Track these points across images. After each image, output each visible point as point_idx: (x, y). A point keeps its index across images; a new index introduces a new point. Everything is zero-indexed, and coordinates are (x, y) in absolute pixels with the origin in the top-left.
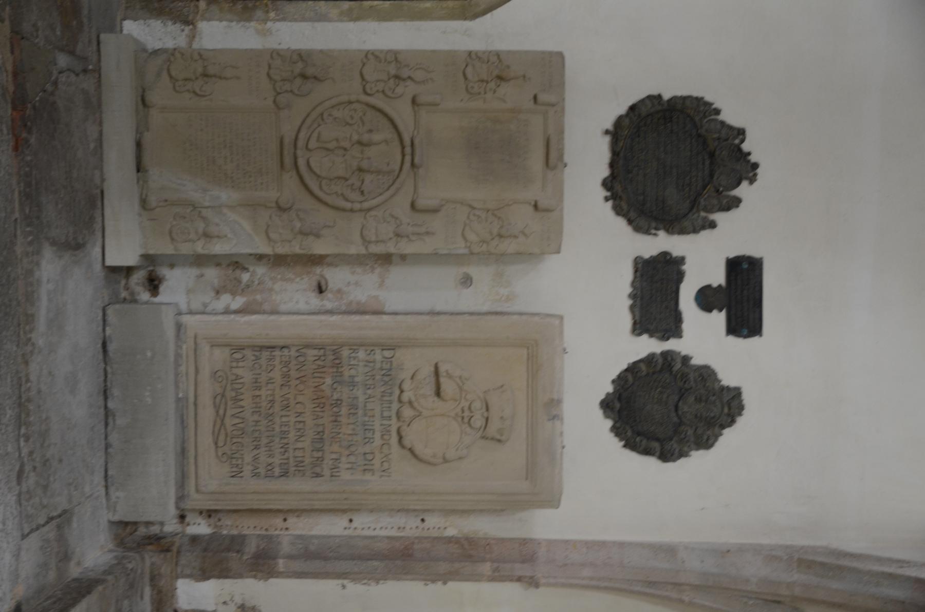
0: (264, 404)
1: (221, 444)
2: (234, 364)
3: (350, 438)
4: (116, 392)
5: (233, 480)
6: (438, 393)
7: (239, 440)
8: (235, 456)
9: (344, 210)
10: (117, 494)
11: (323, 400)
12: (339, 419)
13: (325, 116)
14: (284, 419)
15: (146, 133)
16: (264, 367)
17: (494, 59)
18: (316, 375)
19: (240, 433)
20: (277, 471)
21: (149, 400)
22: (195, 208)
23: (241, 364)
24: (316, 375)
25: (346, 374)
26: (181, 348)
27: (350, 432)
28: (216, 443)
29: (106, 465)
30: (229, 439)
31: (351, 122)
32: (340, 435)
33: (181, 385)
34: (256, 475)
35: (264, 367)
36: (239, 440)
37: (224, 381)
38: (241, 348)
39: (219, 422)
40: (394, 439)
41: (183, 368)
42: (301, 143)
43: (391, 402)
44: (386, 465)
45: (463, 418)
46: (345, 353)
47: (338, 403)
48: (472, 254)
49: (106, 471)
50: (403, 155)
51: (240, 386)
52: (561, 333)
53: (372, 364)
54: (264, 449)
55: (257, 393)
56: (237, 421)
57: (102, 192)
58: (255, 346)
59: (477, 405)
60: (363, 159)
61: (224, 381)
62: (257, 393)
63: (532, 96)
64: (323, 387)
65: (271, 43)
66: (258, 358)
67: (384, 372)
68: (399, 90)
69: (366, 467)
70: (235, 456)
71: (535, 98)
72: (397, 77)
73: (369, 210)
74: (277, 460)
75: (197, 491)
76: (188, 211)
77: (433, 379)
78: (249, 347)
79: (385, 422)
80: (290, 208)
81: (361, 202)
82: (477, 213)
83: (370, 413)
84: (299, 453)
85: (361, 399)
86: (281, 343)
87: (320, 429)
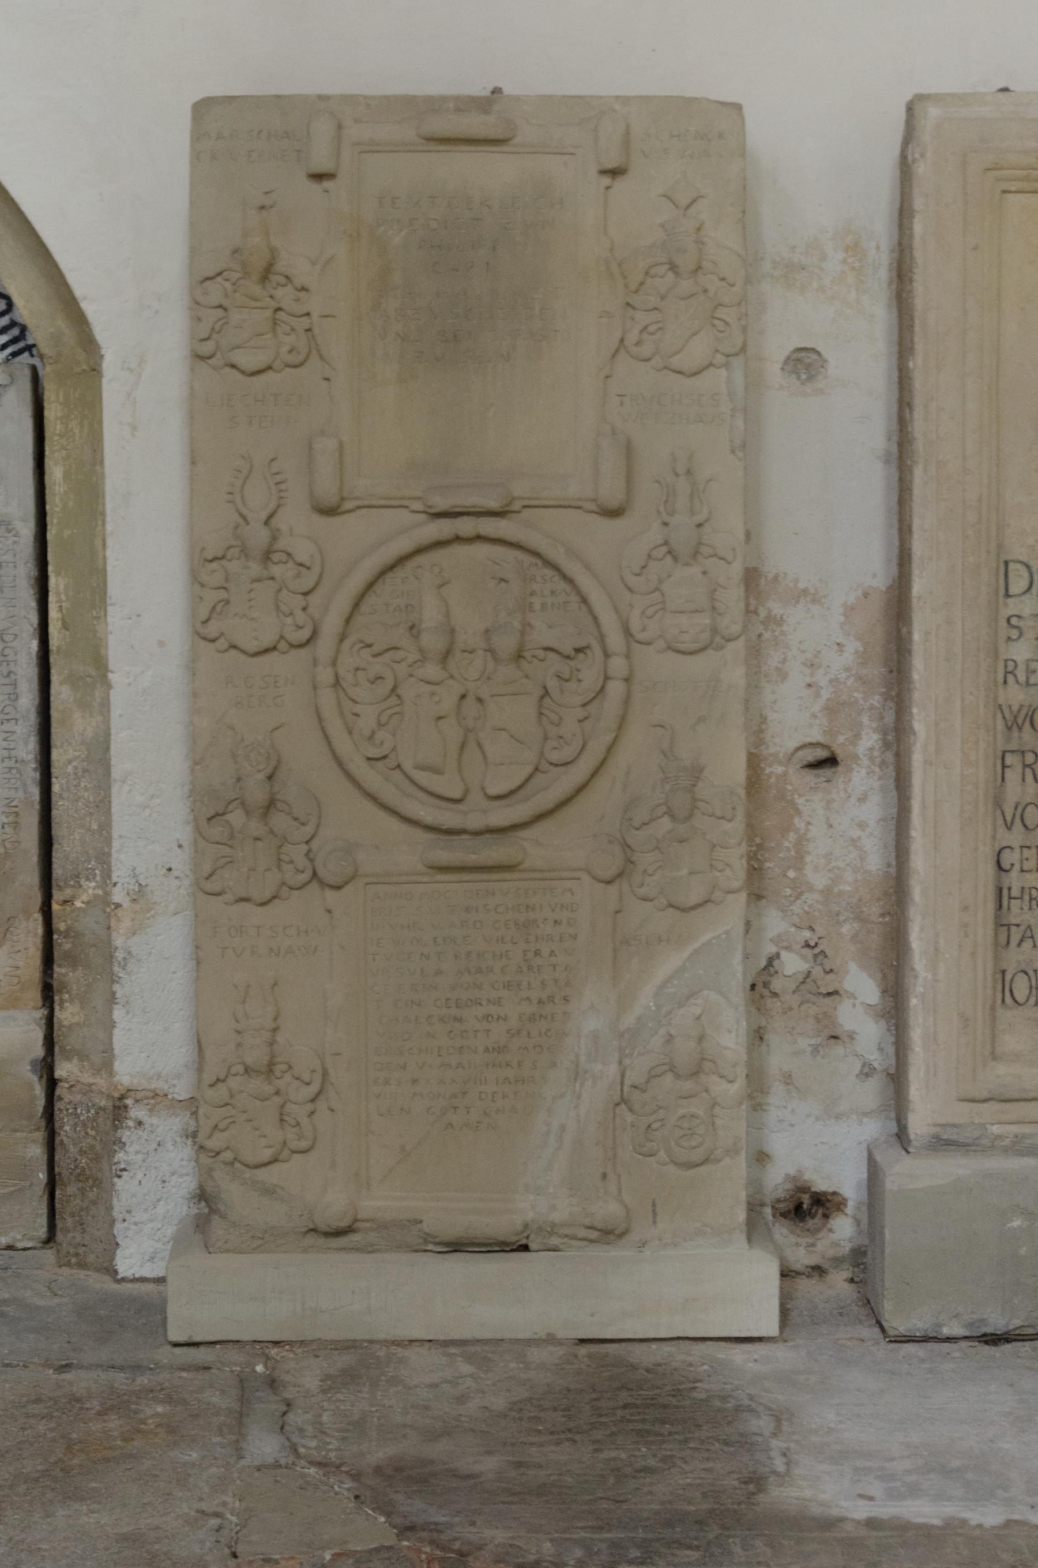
9: (627, 702)
13: (374, 752)
15: (424, 1226)
17: (215, 292)
22: (623, 1100)
26: (998, 1137)
31: (389, 684)
42: (448, 818)
46: (1015, 696)
48: (743, 349)
50: (479, 538)
52: (961, 99)
57: (582, 1341)
58: (996, 944)
60: (490, 650)
63: (315, 187)
65: (173, 896)
68: (303, 551)
71: (319, 177)
72: (267, 557)
73: (627, 632)
76: (630, 1118)
78: (996, 959)
80: (626, 846)
81: (607, 655)
82: (633, 336)
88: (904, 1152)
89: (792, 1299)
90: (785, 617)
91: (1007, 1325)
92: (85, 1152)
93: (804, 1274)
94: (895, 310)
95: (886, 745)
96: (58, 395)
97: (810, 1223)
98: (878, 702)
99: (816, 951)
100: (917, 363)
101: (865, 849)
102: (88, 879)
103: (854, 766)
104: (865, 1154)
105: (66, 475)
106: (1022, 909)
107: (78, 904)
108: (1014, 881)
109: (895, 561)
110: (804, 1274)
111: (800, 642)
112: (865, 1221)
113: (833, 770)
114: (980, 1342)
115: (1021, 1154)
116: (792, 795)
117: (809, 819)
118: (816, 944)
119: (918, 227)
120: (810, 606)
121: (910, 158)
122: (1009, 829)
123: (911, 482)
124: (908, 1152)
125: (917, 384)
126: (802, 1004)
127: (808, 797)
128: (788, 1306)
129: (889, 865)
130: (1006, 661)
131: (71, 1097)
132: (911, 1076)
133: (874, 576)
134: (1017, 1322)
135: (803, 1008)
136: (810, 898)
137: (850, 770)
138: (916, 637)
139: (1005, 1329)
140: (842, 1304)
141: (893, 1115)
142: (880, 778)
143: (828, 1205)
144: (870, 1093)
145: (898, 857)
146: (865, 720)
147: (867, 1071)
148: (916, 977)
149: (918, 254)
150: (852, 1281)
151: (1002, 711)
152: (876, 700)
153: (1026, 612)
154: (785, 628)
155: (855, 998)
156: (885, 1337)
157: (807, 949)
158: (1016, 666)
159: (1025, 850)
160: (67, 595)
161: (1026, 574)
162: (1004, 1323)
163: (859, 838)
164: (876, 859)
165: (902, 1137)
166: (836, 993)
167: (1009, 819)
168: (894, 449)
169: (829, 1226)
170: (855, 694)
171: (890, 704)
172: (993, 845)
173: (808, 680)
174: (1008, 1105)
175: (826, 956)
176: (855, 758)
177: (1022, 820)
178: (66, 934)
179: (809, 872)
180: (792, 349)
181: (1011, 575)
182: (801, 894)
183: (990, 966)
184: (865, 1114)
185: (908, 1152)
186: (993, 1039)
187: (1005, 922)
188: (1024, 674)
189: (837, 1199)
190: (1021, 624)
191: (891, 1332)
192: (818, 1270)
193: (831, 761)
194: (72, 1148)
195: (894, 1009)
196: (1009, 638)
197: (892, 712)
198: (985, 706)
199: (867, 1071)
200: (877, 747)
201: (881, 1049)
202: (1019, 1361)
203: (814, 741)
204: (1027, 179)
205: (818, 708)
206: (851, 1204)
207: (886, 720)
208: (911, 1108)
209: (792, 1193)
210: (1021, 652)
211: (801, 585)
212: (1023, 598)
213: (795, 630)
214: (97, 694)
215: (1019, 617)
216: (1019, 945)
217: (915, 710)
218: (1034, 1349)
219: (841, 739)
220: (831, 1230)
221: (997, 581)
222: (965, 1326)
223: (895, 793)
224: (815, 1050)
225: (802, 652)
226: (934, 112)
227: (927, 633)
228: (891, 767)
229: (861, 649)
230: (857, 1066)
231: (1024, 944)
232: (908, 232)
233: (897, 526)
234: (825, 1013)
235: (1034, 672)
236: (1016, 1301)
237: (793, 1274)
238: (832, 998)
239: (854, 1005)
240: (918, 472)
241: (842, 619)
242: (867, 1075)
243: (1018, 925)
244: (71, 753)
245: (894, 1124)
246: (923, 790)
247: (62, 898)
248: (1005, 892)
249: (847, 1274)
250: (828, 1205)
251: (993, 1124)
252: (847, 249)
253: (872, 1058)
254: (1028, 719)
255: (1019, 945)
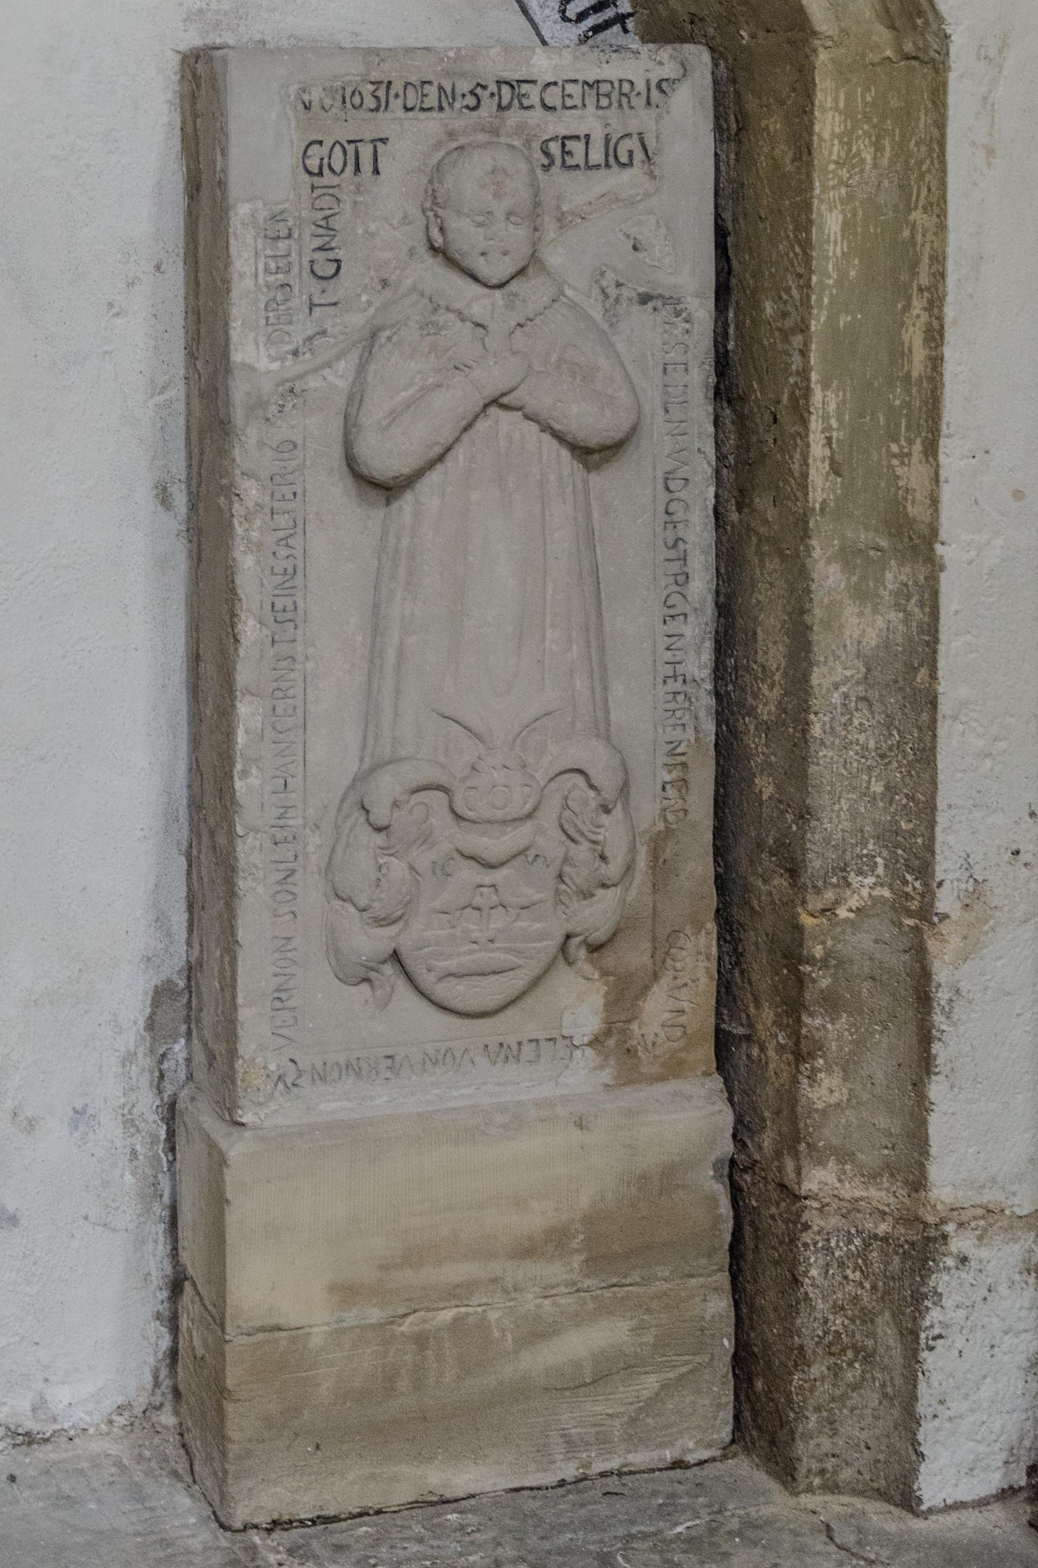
92: (842, 1308)
96: (836, 100)
102: (860, 873)
105: (847, 226)
107: (842, 913)
131: (822, 1223)
160: (840, 420)
178: (824, 963)
194: (820, 1305)
214: (889, 576)
244: (840, 673)
247: (820, 906)
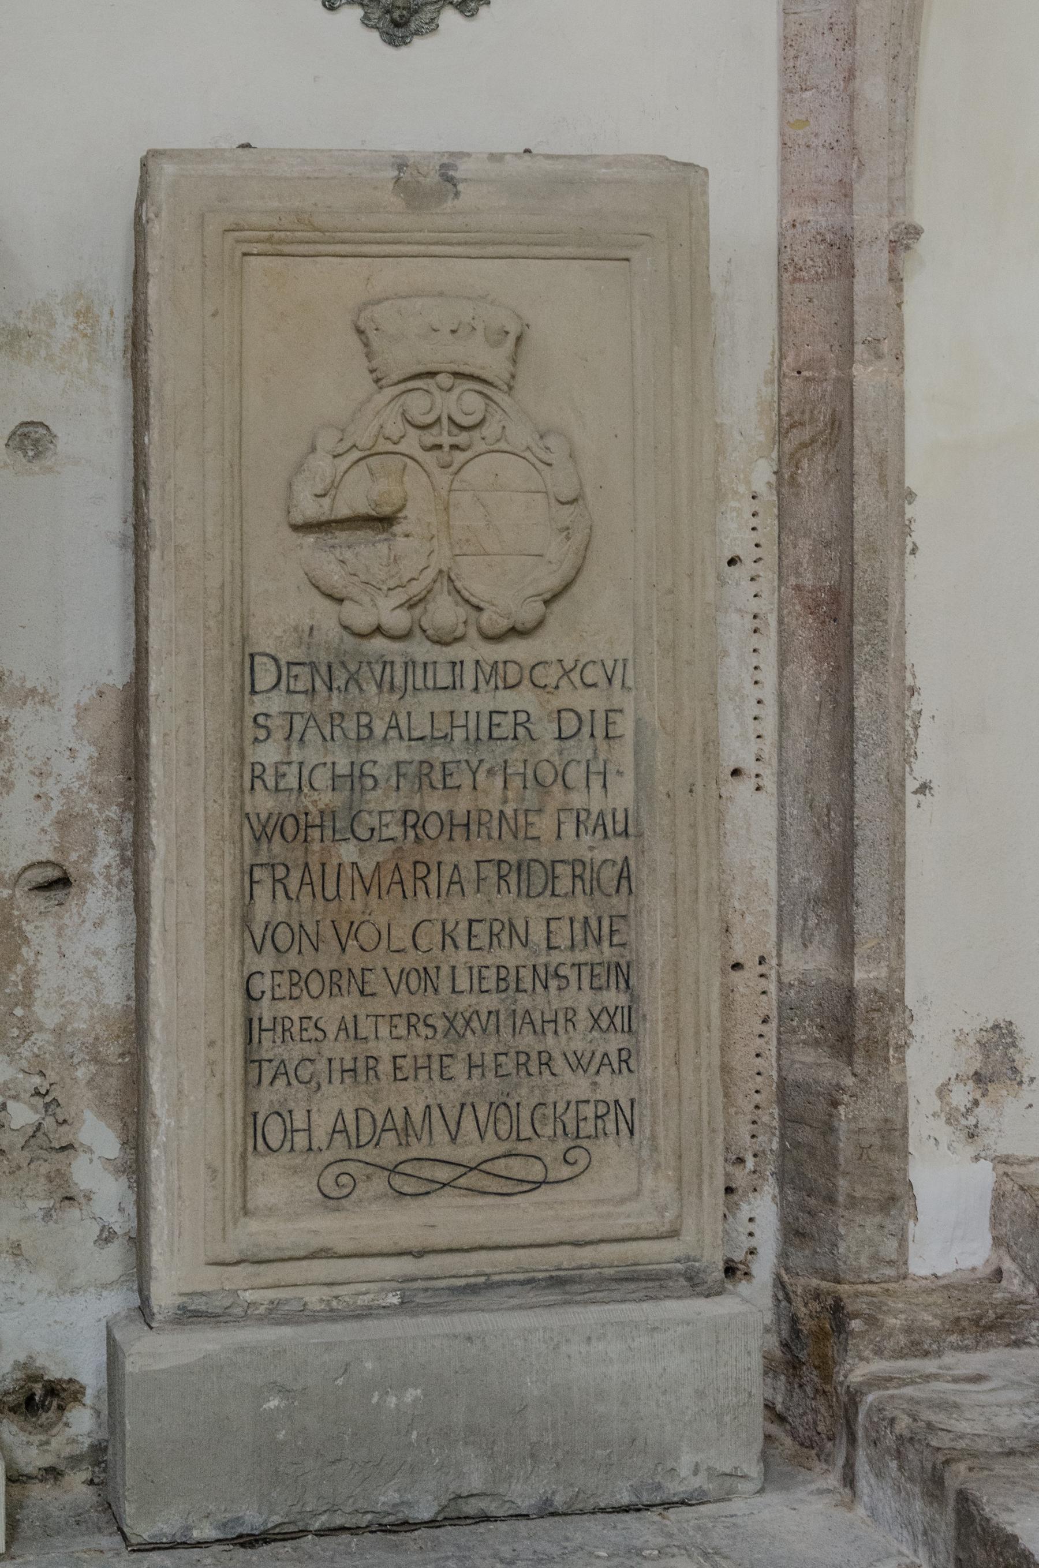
0: (419, 1045)
1: (536, 1171)
2: (301, 1140)
3: (517, 782)
4: (387, 1497)
5: (644, 1128)
6: (382, 522)
7: (525, 1114)
8: (571, 1128)
10: (684, 1471)
11: (407, 866)
12: (460, 818)
14: (463, 984)
16: (309, 1050)
18: (330, 892)
19: (502, 1112)
20: (614, 998)
21: (412, 1394)
23: (300, 1123)
24: (330, 892)
25: (326, 798)
27: (499, 782)
28: (539, 1184)
29: (603, 1511)
30: (522, 1147)
32: (509, 812)
33: (361, 1301)
34: (626, 1060)
35: (309, 1050)
36: (525, 1114)
37: (351, 1167)
38: (253, 1124)
39: (472, 1179)
40: (518, 650)
41: (314, 1297)
43: (410, 664)
44: (592, 674)
45: (454, 447)
46: (263, 803)
47: (413, 821)
49: (626, 1510)
51: (365, 1119)
52: (199, 155)
53: (299, 723)
54: (550, 1039)
55: (385, 1067)
56: (468, 1124)
58: (246, 1083)
59: (418, 405)
61: (351, 1167)
62: (385, 1067)
64: (367, 868)
66: (281, 1071)
67: (318, 683)
69: (599, 732)
70: (571, 1128)
74: (583, 1000)
75: (674, 1234)
77: (342, 536)
79: (469, 681)
83: (443, 725)
84: (562, 939)
85: (399, 751)
86: (235, 1000)
87: (490, 872)
88: (146, 1328)
89: (22, 1507)
90: (10, 721)
91: (265, 1522)
93: (36, 1477)
94: (130, 381)
95: (124, 861)
97: (44, 1418)
98: (115, 813)
99: (48, 1099)
100: (153, 438)
101: (101, 980)
103: (89, 886)
104: (105, 1333)
106: (274, 1042)
108: (266, 1010)
109: (131, 657)
110: (36, 1477)
111: (28, 748)
112: (105, 1411)
113: (65, 892)
114: (235, 1545)
115: (278, 1323)
116: (20, 922)
117: (38, 948)
118: (48, 1091)
119: (153, 291)
120: (38, 706)
121: (144, 218)
122: (259, 952)
123: (148, 568)
124: (151, 1328)
125: (153, 462)
126: (31, 1161)
127: (38, 924)
128: (18, 1517)
129: (129, 998)
130: (253, 764)
132: (153, 1240)
133: (110, 672)
134: (276, 1519)
135: (32, 1166)
136: (42, 1039)
137: (84, 891)
138: (154, 740)
139: (262, 1528)
140: (80, 1511)
141: (135, 1287)
142: (117, 900)
143: (63, 1395)
144: (111, 1261)
145: (137, 988)
146: (101, 833)
147: (106, 1236)
148: (157, 1124)
149: (152, 320)
150: (91, 1482)
151: (249, 819)
152: (113, 812)
153: (274, 710)
154: (11, 732)
155: (92, 1152)
156: (127, 1546)
157: (37, 1098)
158: (264, 770)
159: (277, 976)
161: (273, 668)
162: (261, 1520)
163: (96, 968)
164: (115, 994)
165: (144, 1311)
166: (70, 1146)
167: (258, 941)
168: (131, 532)
169: (64, 1419)
170: (90, 805)
171: (129, 815)
172: (242, 972)
173: (37, 790)
174: (262, 1268)
175: (59, 1105)
176: (90, 877)
177: (273, 941)
179: (38, 1008)
180: (17, 424)
181: (257, 668)
182: (30, 1034)
183: (240, 1107)
184: (104, 1286)
185: (151, 1328)
186: (244, 1193)
187: (257, 1058)
188: (273, 779)
189: (73, 1387)
190: (269, 723)
191: (134, 1540)
192: (53, 1473)
193: (63, 882)
195: (135, 1167)
196: (256, 739)
197: (131, 824)
198: (231, 816)
199: (106, 1236)
200: (114, 864)
201: (121, 1210)
202: (278, 1563)
203: (44, 860)
204: (269, 240)
205: (49, 822)
206: (89, 1392)
207: (124, 833)
208: (153, 1276)
209: (22, 1383)
210: (269, 754)
211: (29, 685)
212: (270, 695)
213: (21, 735)
215: (266, 715)
216: (272, 1083)
217: (153, 822)
218: (295, 1549)
219: (74, 856)
220: (67, 1425)
221: (242, 675)
222: (218, 1528)
223: (134, 916)
224: (48, 1215)
225: (31, 759)
226: (168, 169)
227: (165, 735)
228: (131, 887)
229: (96, 755)
230: (96, 1229)
231: (277, 1082)
232: (142, 297)
233: (133, 617)
234: (58, 1170)
235: (284, 775)
236: (274, 1494)
237: (24, 1478)
238: (66, 1153)
239: (91, 1161)
240: (155, 556)
241: (75, 721)
242: (107, 1240)
243: (270, 1061)
245: (137, 1295)
246: (163, 911)
248: (256, 1025)
249: (85, 1475)
250: (63, 1395)
251: (245, 1290)
252: (77, 316)
253: (112, 1220)
254: (278, 829)
255: (272, 1083)
